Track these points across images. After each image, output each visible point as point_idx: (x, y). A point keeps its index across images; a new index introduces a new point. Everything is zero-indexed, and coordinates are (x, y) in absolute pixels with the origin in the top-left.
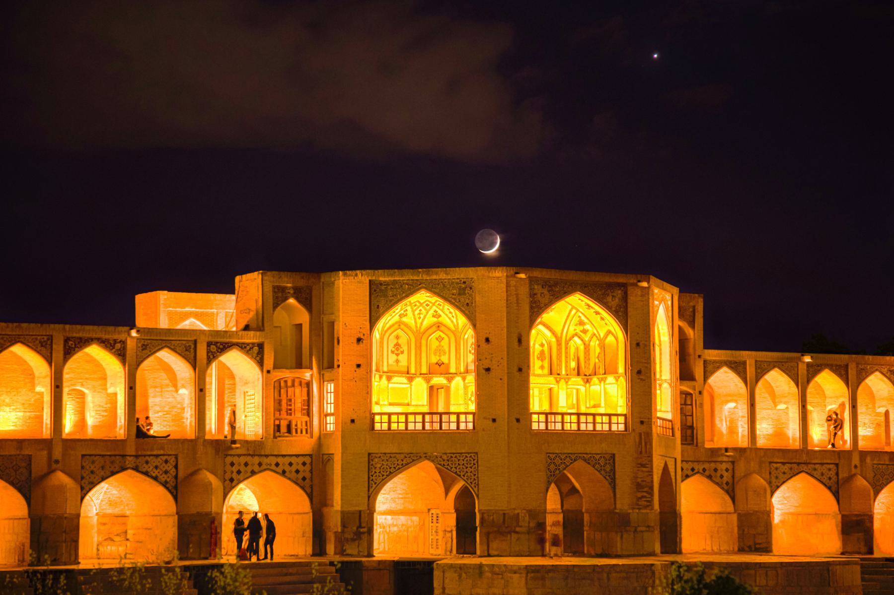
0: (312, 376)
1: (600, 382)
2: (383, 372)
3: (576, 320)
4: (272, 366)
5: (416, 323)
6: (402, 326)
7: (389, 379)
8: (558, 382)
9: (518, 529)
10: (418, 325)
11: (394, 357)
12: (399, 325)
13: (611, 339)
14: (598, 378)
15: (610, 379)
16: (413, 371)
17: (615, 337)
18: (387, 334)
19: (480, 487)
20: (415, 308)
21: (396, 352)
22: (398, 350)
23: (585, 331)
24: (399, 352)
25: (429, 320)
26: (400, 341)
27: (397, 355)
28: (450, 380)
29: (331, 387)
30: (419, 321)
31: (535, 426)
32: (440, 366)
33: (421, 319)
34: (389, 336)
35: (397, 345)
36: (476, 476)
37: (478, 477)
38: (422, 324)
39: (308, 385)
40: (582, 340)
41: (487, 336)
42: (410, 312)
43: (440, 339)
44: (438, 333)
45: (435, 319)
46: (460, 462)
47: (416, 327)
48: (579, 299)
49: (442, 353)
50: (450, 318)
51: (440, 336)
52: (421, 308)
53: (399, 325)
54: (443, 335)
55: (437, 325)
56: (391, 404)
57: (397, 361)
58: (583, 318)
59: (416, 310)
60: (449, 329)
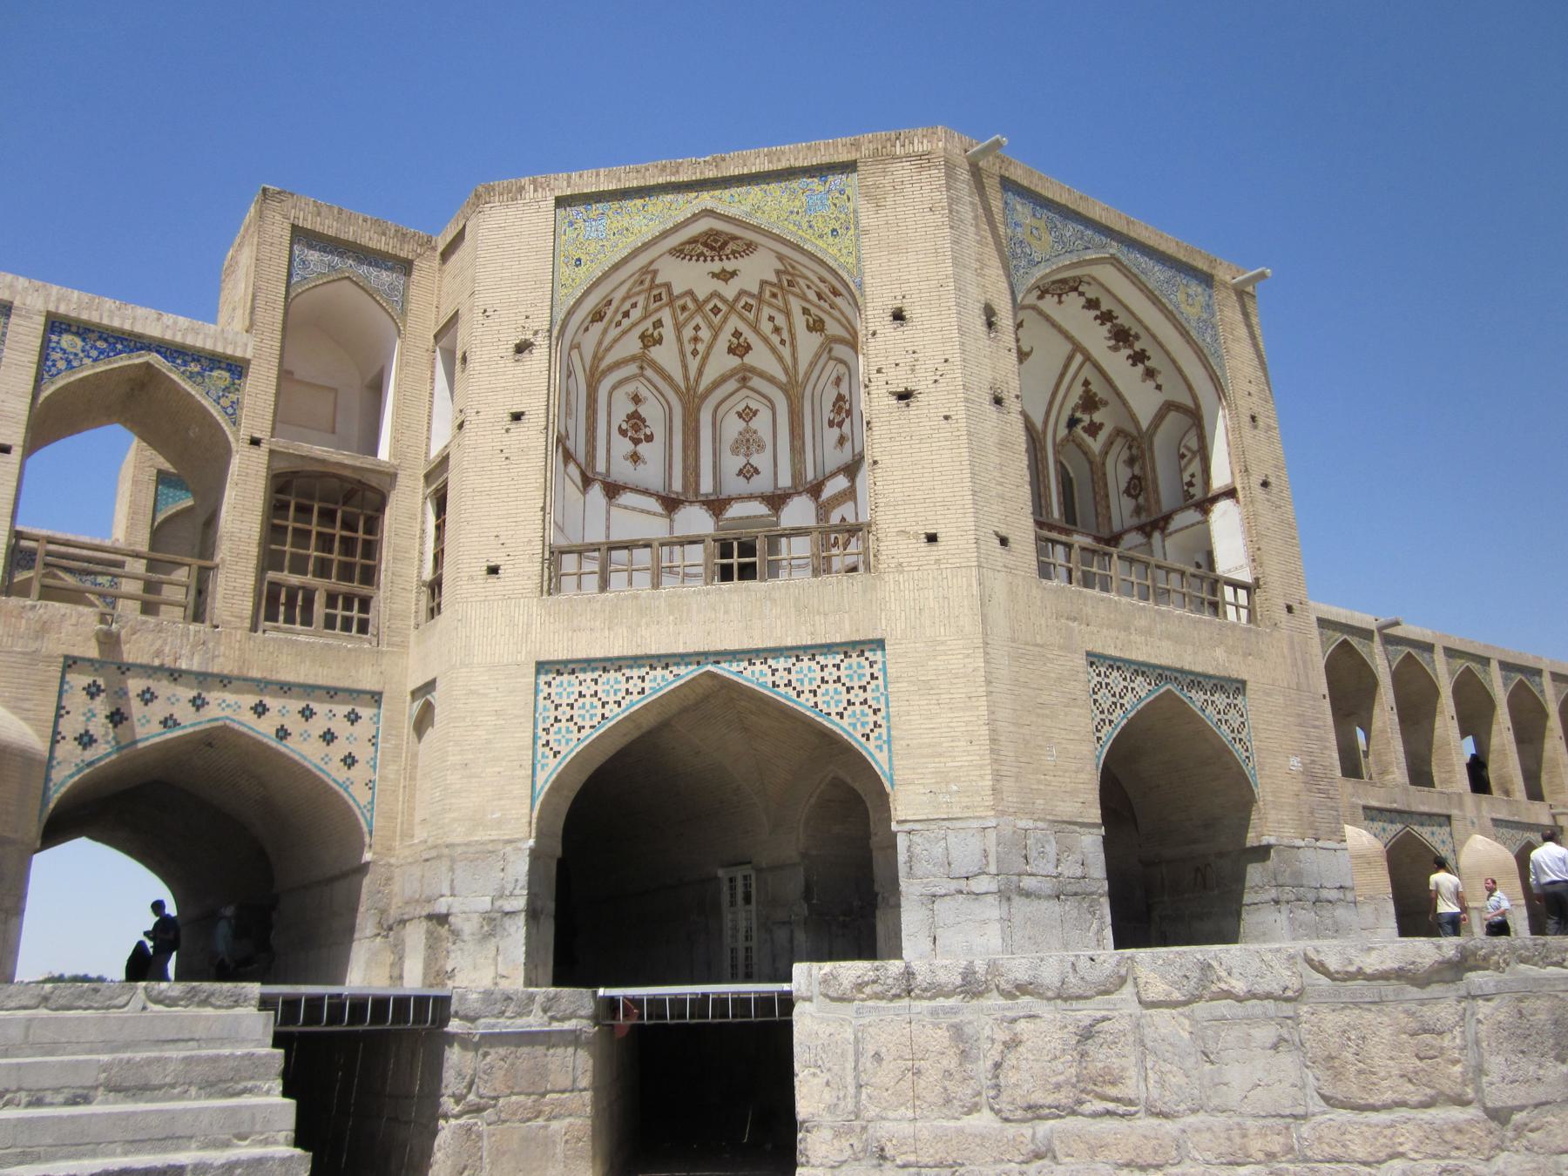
1: (1149, 536)
4: (268, 424)
6: (649, 372)
9: (1027, 883)
19: (896, 747)
20: (681, 318)
22: (636, 428)
26: (643, 410)
27: (636, 442)
30: (693, 364)
32: (748, 479)
33: (699, 357)
34: (614, 388)
35: (636, 419)
36: (883, 713)
37: (888, 717)
40: (1085, 453)
41: (898, 304)
42: (668, 331)
43: (747, 414)
44: (740, 402)
46: (825, 674)
50: (773, 350)
52: (698, 320)
55: (741, 375)
59: (684, 325)
60: (772, 380)
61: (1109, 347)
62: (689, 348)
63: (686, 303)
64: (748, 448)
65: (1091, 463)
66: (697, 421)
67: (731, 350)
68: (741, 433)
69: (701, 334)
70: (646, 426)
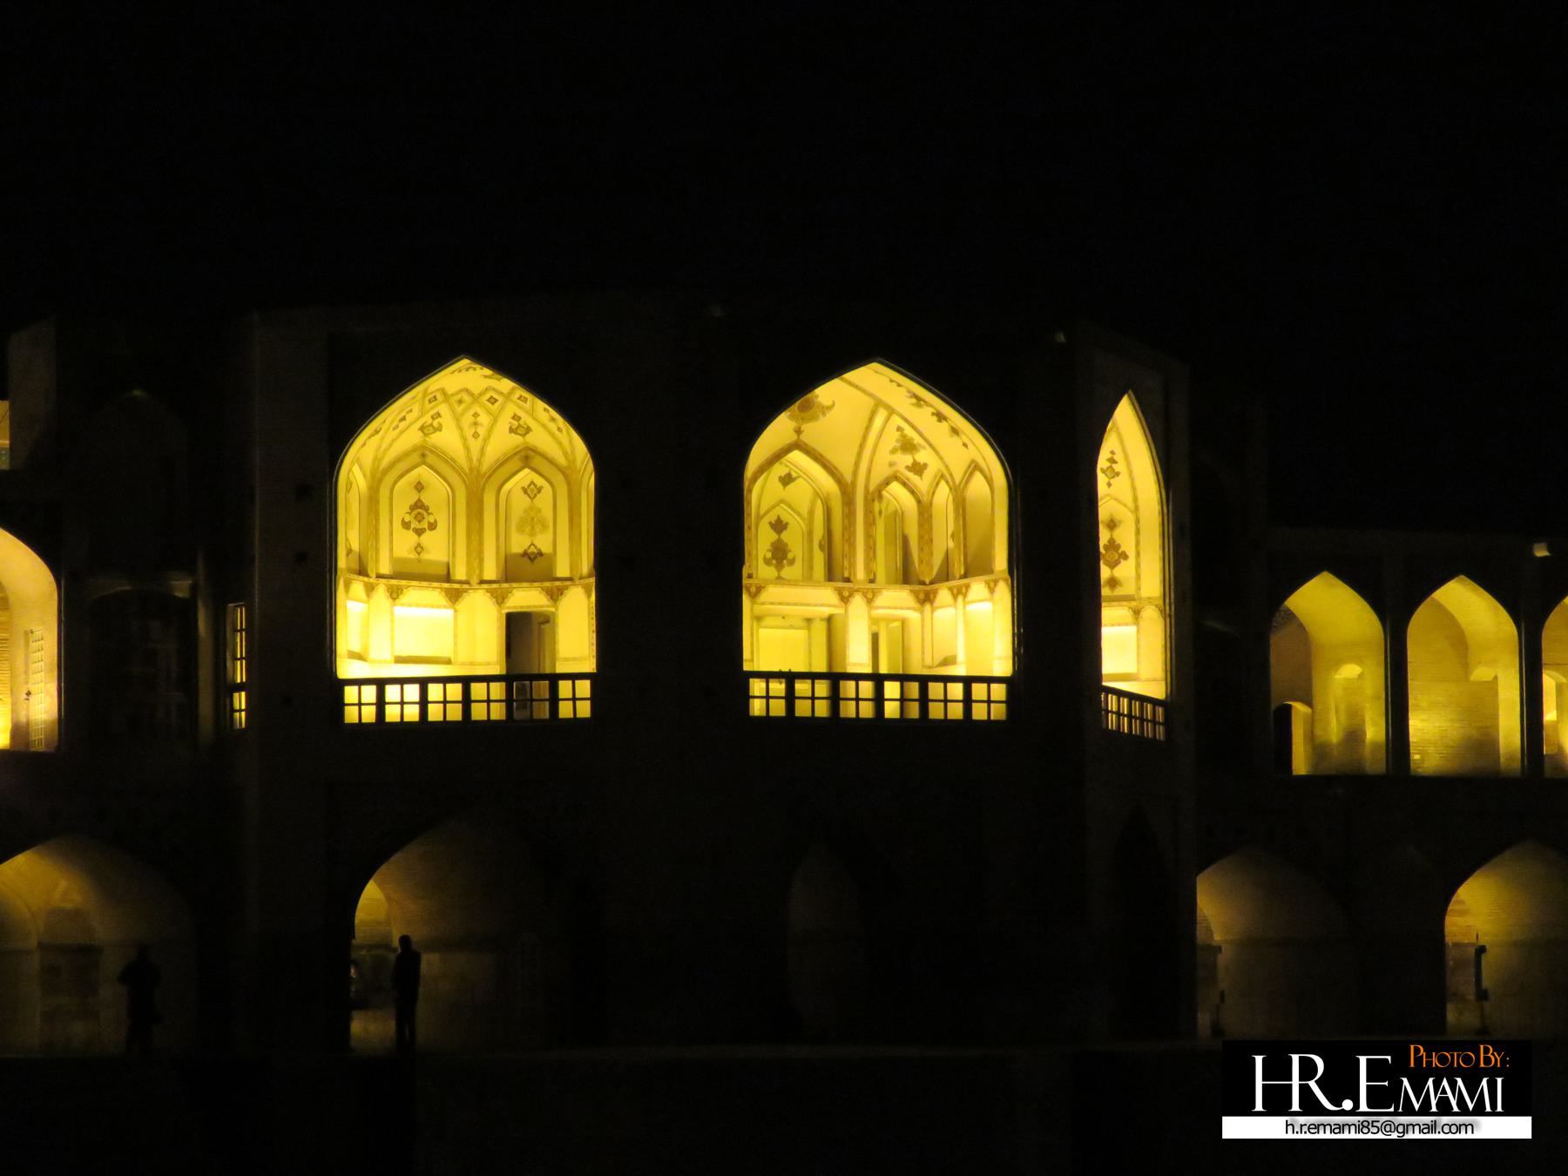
0: (194, 589)
1: (955, 598)
2: (379, 576)
3: (891, 439)
5: (467, 449)
7: (394, 594)
8: (845, 600)
10: (475, 454)
11: (411, 538)
12: (423, 455)
13: (978, 484)
14: (951, 589)
15: (978, 587)
16: (460, 573)
17: (985, 477)
18: (389, 479)
21: (415, 525)
22: (420, 518)
23: (918, 468)
24: (425, 525)
25: (502, 442)
26: (426, 498)
27: (419, 532)
28: (555, 595)
29: (240, 616)
30: (475, 446)
31: (757, 708)
35: (419, 507)
38: (482, 450)
39: (186, 611)
40: (913, 492)
42: (447, 419)
43: (531, 491)
44: (525, 476)
45: (516, 440)
47: (470, 459)
48: (891, 381)
49: (538, 528)
50: (552, 434)
51: (532, 483)
53: (423, 455)
54: (539, 481)
56: (400, 660)
57: (419, 548)
58: (909, 432)
59: (462, 414)
60: (552, 462)
61: (913, 404)
62: (469, 432)
63: (462, 397)
64: (533, 527)
65: (919, 502)
66: (481, 502)
67: (512, 430)
68: (525, 511)
69: (480, 419)
70: (429, 514)
